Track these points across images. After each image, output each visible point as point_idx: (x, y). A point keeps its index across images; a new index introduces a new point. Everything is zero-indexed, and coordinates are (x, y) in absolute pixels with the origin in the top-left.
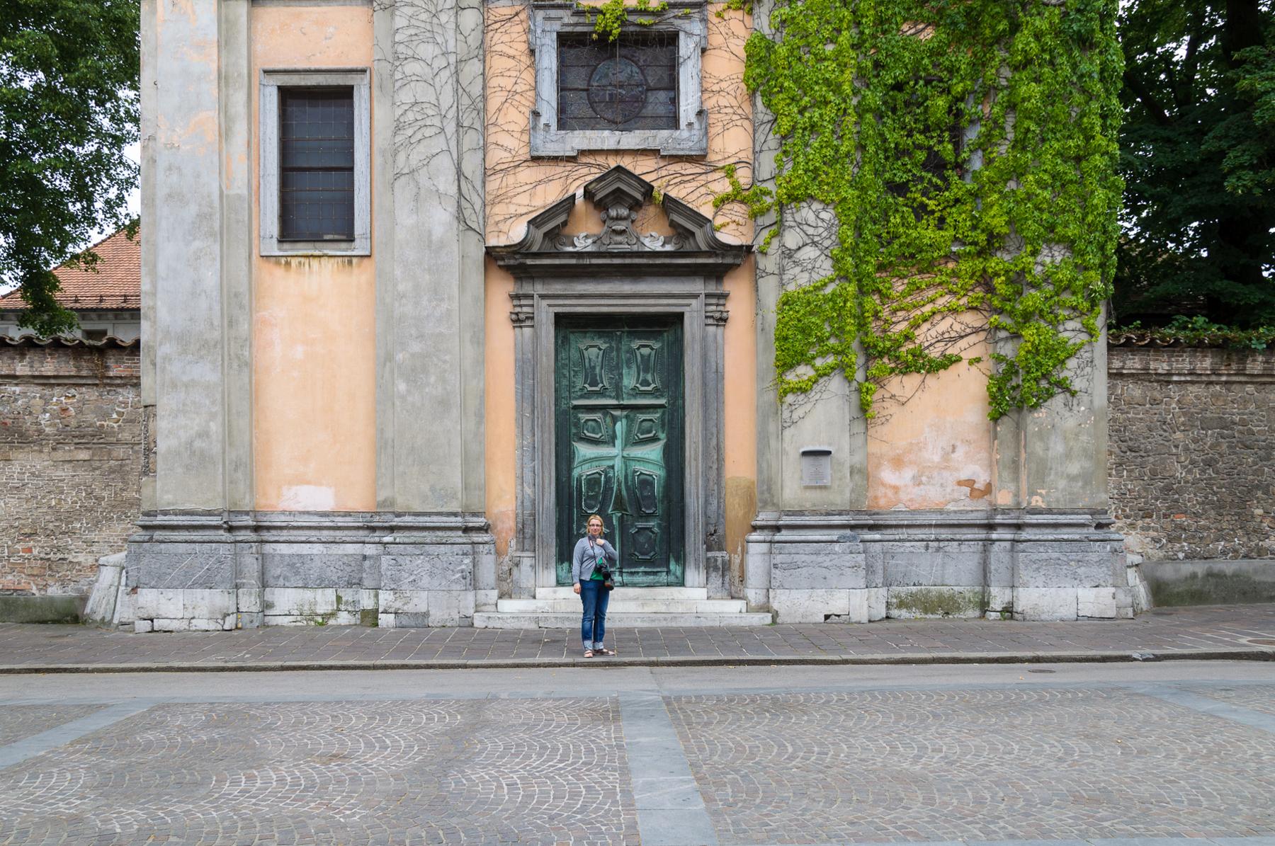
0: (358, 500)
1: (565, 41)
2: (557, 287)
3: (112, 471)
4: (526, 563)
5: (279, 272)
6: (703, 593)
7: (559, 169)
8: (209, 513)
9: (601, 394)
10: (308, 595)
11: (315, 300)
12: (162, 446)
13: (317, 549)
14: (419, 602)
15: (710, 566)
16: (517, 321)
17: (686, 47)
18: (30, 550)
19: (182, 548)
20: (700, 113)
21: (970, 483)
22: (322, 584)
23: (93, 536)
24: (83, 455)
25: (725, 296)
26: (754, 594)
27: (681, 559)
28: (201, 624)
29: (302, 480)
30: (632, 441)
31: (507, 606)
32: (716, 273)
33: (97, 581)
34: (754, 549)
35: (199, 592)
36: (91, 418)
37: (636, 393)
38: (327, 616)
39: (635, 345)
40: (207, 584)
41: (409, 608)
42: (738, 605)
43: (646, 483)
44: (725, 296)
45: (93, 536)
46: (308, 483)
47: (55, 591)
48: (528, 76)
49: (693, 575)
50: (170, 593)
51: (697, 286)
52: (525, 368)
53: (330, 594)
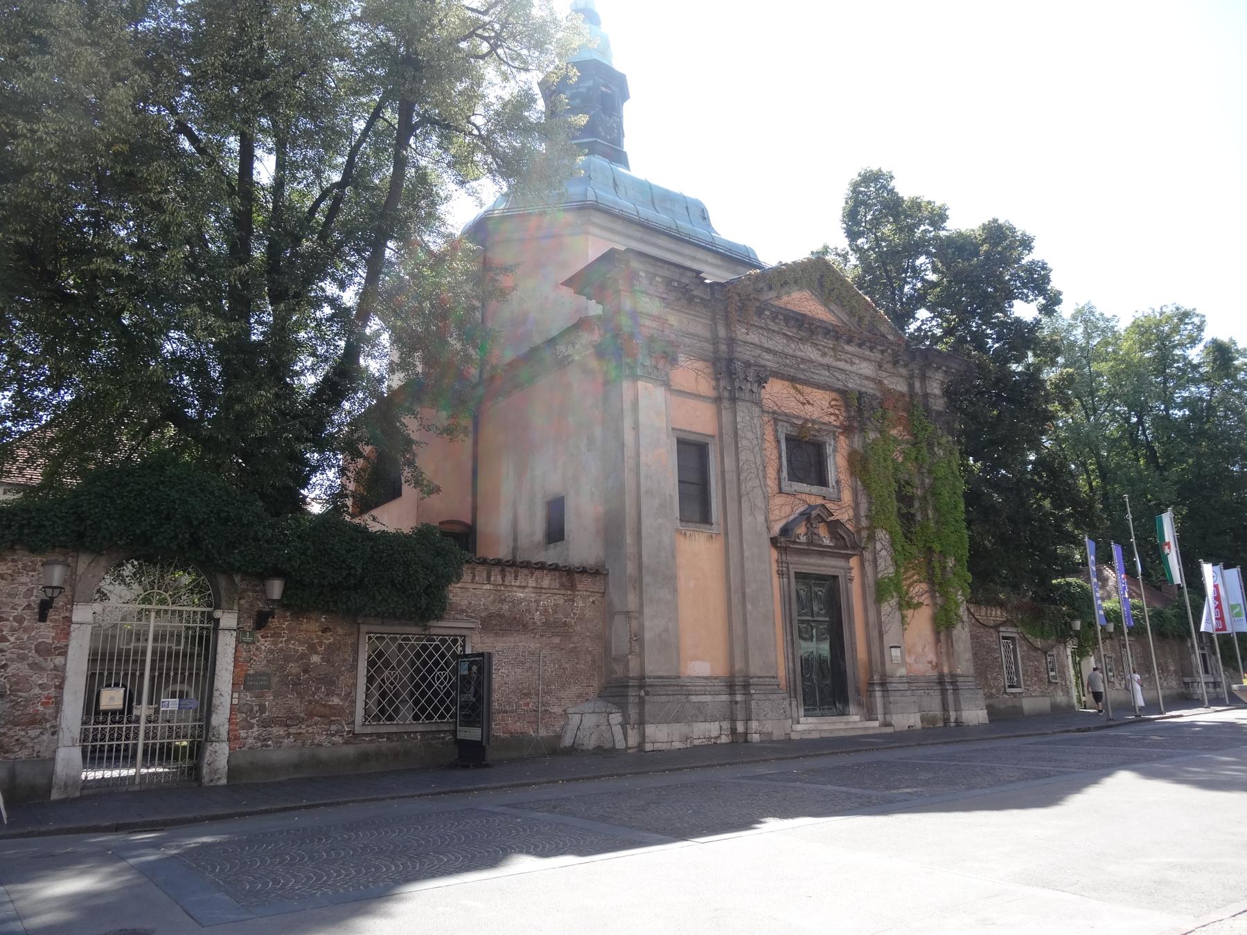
0: (721, 670)
1: (789, 439)
2: (795, 558)
3: (571, 651)
4: (794, 703)
5: (682, 538)
6: (857, 718)
7: (790, 499)
8: (669, 677)
9: (806, 615)
10: (706, 726)
11: (698, 556)
12: (648, 636)
13: (708, 698)
14: (769, 727)
15: (860, 705)
16: (781, 574)
17: (829, 450)
18: (527, 704)
19: (664, 698)
20: (838, 482)
21: (930, 662)
22: (714, 719)
23: (561, 694)
24: (557, 640)
25: (851, 569)
26: (880, 717)
27: (846, 702)
28: (677, 745)
29: (695, 658)
30: (819, 640)
31: (799, 727)
32: (847, 557)
33: (567, 724)
34: (878, 694)
35: (676, 726)
36: (560, 616)
37: (818, 614)
38: (717, 738)
39: (816, 589)
40: (677, 720)
41: (765, 730)
42: (876, 724)
43: (825, 661)
44: (851, 569)
45: (561, 694)
46: (699, 659)
47: (543, 733)
48: (775, 452)
49: (852, 708)
50: (660, 726)
51: (840, 563)
52: (786, 601)
53: (717, 723)
